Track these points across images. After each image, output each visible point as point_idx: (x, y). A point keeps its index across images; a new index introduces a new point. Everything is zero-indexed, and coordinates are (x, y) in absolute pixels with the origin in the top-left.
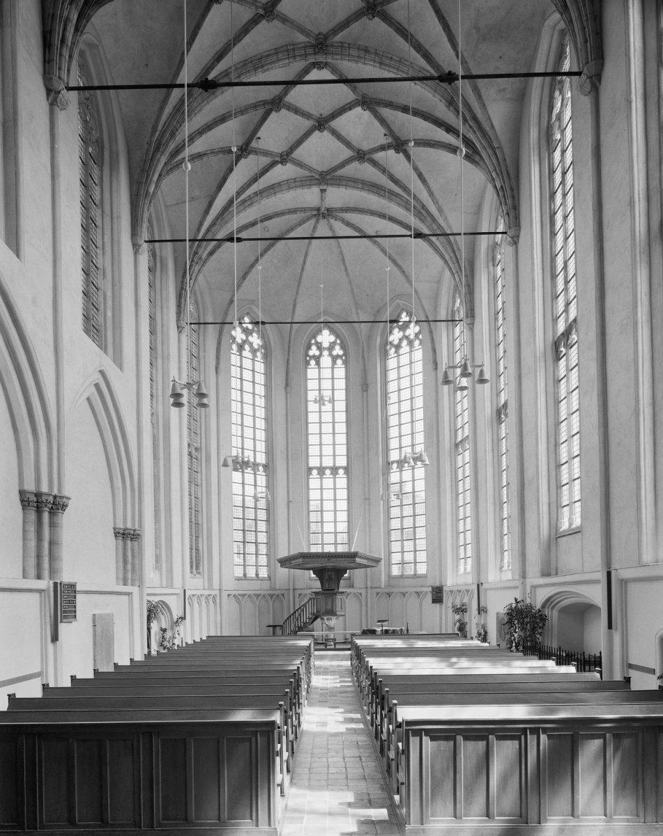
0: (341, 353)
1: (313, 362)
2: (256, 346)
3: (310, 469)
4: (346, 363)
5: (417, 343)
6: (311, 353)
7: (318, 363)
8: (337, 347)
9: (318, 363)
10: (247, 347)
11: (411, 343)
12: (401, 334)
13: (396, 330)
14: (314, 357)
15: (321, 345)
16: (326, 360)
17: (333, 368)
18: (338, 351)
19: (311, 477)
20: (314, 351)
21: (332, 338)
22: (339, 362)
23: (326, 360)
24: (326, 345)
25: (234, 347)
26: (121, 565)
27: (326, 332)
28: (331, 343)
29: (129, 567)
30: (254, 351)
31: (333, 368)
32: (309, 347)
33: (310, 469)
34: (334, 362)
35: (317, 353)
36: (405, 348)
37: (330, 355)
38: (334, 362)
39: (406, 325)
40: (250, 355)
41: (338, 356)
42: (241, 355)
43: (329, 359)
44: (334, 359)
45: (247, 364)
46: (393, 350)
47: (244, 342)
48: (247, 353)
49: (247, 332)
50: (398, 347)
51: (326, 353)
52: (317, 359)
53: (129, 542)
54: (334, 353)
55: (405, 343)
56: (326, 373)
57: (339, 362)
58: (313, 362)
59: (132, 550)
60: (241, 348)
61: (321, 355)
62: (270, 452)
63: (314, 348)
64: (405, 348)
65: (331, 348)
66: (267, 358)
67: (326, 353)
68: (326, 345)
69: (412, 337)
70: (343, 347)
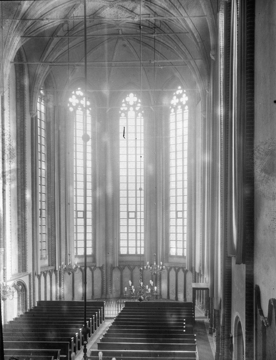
1: (123, 115)
5: (186, 107)
6: (122, 109)
7: (126, 116)
11: (183, 108)
12: (177, 101)
13: (175, 97)
14: (123, 111)
15: (129, 103)
16: (131, 113)
17: (136, 118)
20: (123, 108)
21: (135, 99)
23: (131, 113)
24: (131, 103)
27: (131, 95)
28: (134, 102)
31: (136, 118)
32: (120, 105)
35: (126, 109)
36: (180, 110)
37: (134, 110)
38: (136, 115)
39: (179, 96)
44: (137, 113)
46: (173, 110)
50: (176, 108)
51: (131, 109)
52: (126, 112)
55: (179, 107)
61: (128, 110)
63: (124, 105)
64: (180, 110)
65: (134, 106)
67: (131, 109)
68: (131, 103)
69: (184, 103)
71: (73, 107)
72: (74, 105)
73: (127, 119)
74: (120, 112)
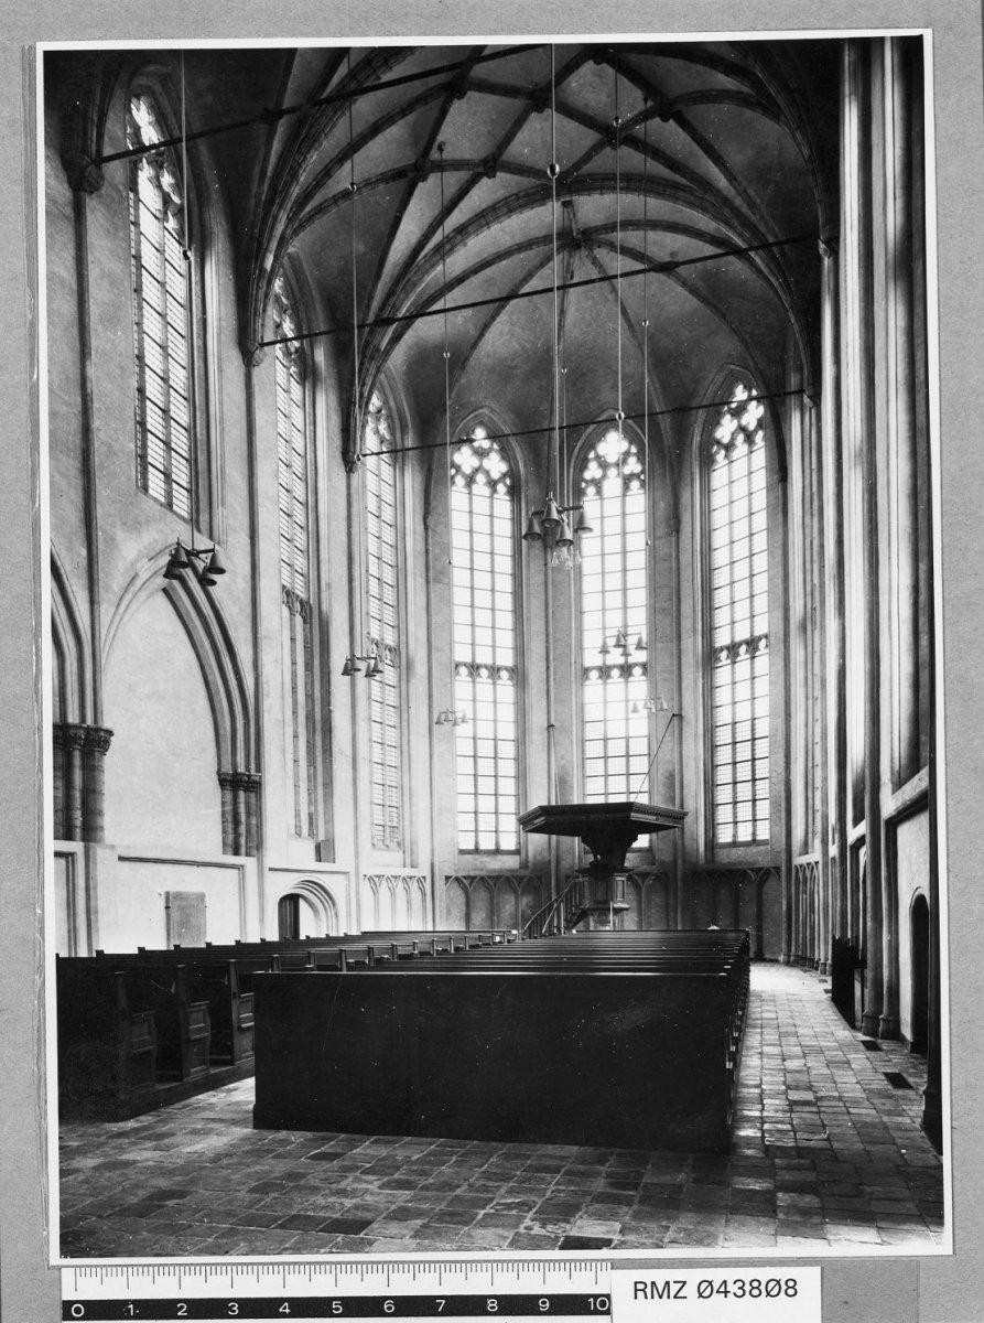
0: (637, 468)
1: (591, 490)
2: (495, 475)
3: (586, 671)
4: (643, 484)
6: (587, 475)
7: (599, 492)
8: (632, 460)
9: (599, 492)
10: (481, 478)
16: (613, 484)
17: (624, 495)
18: (633, 466)
19: (587, 683)
20: (593, 471)
21: (624, 445)
22: (635, 484)
23: (613, 484)
24: (612, 458)
25: (460, 481)
26: (230, 826)
29: (243, 829)
30: (492, 484)
31: (624, 495)
32: (583, 464)
33: (586, 671)
34: (626, 487)
38: (626, 487)
40: (487, 491)
41: (632, 476)
42: (470, 493)
43: (619, 482)
45: (481, 505)
47: (477, 470)
48: (480, 486)
49: (481, 454)
52: (597, 483)
53: (242, 794)
54: (627, 470)
56: (612, 507)
57: (635, 484)
58: (591, 490)
59: (247, 804)
60: (470, 480)
61: (604, 476)
62: (520, 650)
66: (514, 492)
67: (612, 472)
68: (612, 458)
70: (640, 456)
71: (464, 475)
72: (467, 470)
73: (602, 499)
74: (583, 485)
